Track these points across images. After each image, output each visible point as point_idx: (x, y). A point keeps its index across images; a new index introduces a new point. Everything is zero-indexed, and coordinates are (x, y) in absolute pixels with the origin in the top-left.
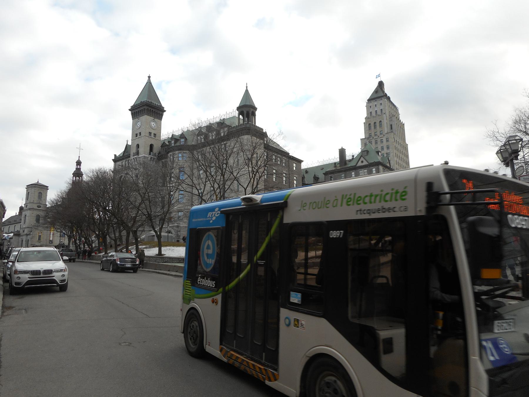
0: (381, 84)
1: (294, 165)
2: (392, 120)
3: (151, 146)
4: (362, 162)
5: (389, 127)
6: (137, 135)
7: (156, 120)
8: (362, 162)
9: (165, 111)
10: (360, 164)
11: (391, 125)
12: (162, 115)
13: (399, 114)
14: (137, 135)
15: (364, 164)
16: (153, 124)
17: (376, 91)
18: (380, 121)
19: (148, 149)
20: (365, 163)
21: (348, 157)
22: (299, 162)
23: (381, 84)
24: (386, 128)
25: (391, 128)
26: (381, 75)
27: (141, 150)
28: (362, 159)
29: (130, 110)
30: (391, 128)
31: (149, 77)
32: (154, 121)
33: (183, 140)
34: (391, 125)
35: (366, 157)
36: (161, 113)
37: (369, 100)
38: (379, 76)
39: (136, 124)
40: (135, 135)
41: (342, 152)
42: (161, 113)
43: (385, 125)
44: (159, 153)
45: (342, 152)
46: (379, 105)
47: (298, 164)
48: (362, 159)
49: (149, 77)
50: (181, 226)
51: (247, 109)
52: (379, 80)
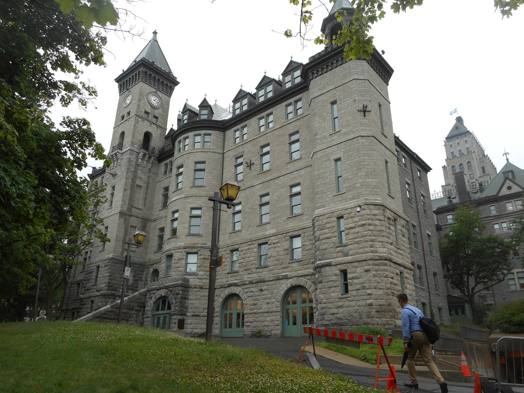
0: (459, 120)
2: (483, 162)
3: (147, 136)
4: (509, 188)
5: (481, 170)
6: (123, 117)
8: (509, 188)
9: (177, 83)
10: (505, 192)
11: (483, 168)
12: (172, 89)
14: (123, 117)
15: (513, 191)
16: (154, 100)
17: (456, 127)
18: (469, 162)
19: (141, 138)
23: (459, 120)
24: (477, 170)
25: (484, 171)
26: (458, 110)
27: (127, 140)
29: (118, 80)
30: (484, 171)
31: (155, 33)
33: (205, 112)
34: (483, 168)
37: (448, 138)
38: (455, 111)
39: (125, 99)
40: (120, 118)
42: (169, 85)
43: (477, 167)
44: (163, 149)
46: (462, 145)
48: (508, 183)
49: (155, 33)
52: (456, 115)
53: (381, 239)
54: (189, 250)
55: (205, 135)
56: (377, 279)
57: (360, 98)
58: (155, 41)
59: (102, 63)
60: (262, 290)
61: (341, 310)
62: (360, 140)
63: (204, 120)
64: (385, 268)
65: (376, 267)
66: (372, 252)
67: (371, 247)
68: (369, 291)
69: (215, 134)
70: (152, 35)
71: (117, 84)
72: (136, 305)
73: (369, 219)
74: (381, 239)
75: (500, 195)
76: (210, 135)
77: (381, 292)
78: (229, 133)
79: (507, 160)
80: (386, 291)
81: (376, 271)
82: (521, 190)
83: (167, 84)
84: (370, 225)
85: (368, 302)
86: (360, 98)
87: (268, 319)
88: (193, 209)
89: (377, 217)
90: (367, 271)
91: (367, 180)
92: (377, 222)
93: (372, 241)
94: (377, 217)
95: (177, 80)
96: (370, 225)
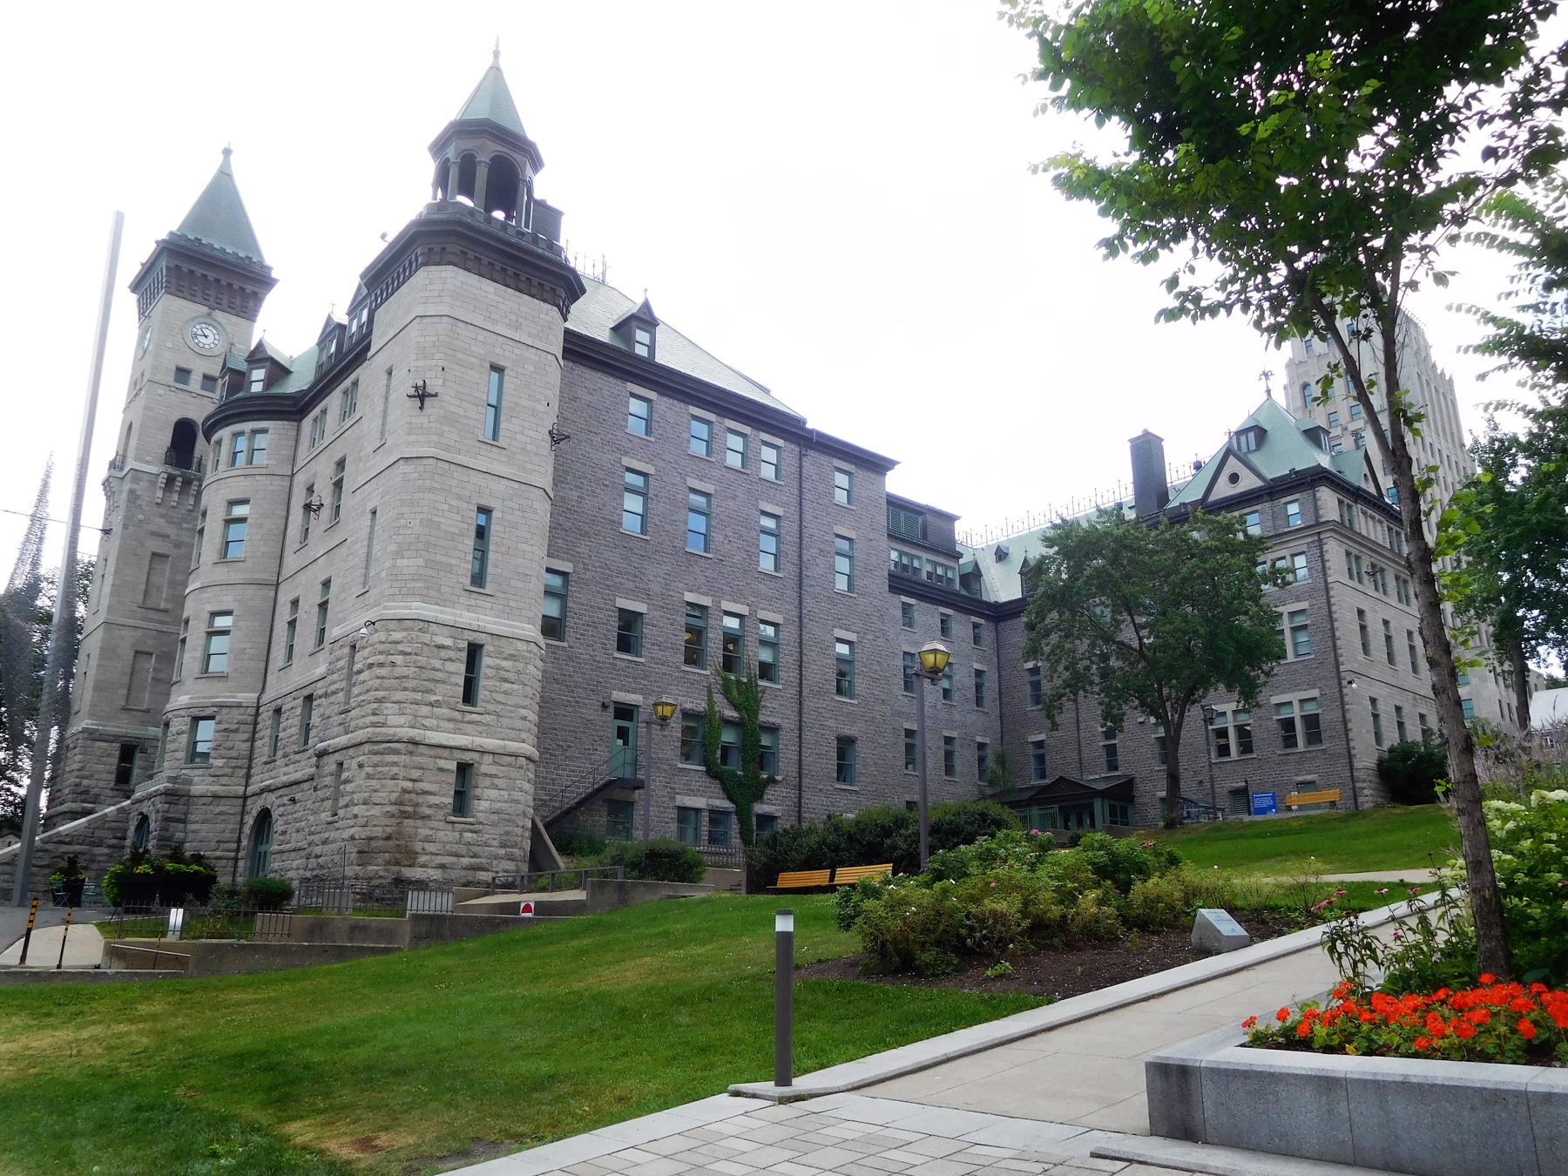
1: (841, 480)
4: (1234, 478)
7: (218, 314)
8: (1234, 478)
10: (1224, 490)
12: (257, 298)
13: (1427, 347)
19: (166, 438)
20: (1249, 482)
21: (1178, 471)
22: (877, 465)
28: (1233, 465)
31: (227, 152)
32: (210, 321)
33: (259, 374)
35: (1255, 459)
36: (249, 288)
41: (1147, 453)
42: (249, 288)
45: (1147, 453)
47: (860, 474)
48: (1233, 465)
49: (227, 152)
50: (196, 789)
51: (469, 144)
53: (399, 696)
54: (196, 712)
55: (255, 432)
56: (373, 782)
57: (421, 363)
58: (224, 174)
59: (221, 200)
60: (293, 800)
61: (326, 848)
62: (402, 467)
63: (258, 397)
64: (394, 758)
65: (376, 758)
66: (374, 725)
67: (374, 714)
68: (356, 810)
69: (276, 429)
70: (222, 157)
71: (134, 297)
72: (109, 834)
73: (381, 653)
74: (399, 696)
75: (1212, 498)
76: (265, 431)
77: (376, 811)
78: (307, 422)
79: (1269, 392)
80: (389, 808)
81: (376, 766)
82: (1260, 483)
83: (242, 289)
84: (381, 665)
85: (352, 831)
86: (421, 363)
87: (294, 865)
88: (214, 614)
89: (400, 647)
90: (361, 766)
91: (399, 562)
92: (399, 659)
93: (380, 701)
94: (400, 647)
95: (274, 275)
96: (381, 665)
